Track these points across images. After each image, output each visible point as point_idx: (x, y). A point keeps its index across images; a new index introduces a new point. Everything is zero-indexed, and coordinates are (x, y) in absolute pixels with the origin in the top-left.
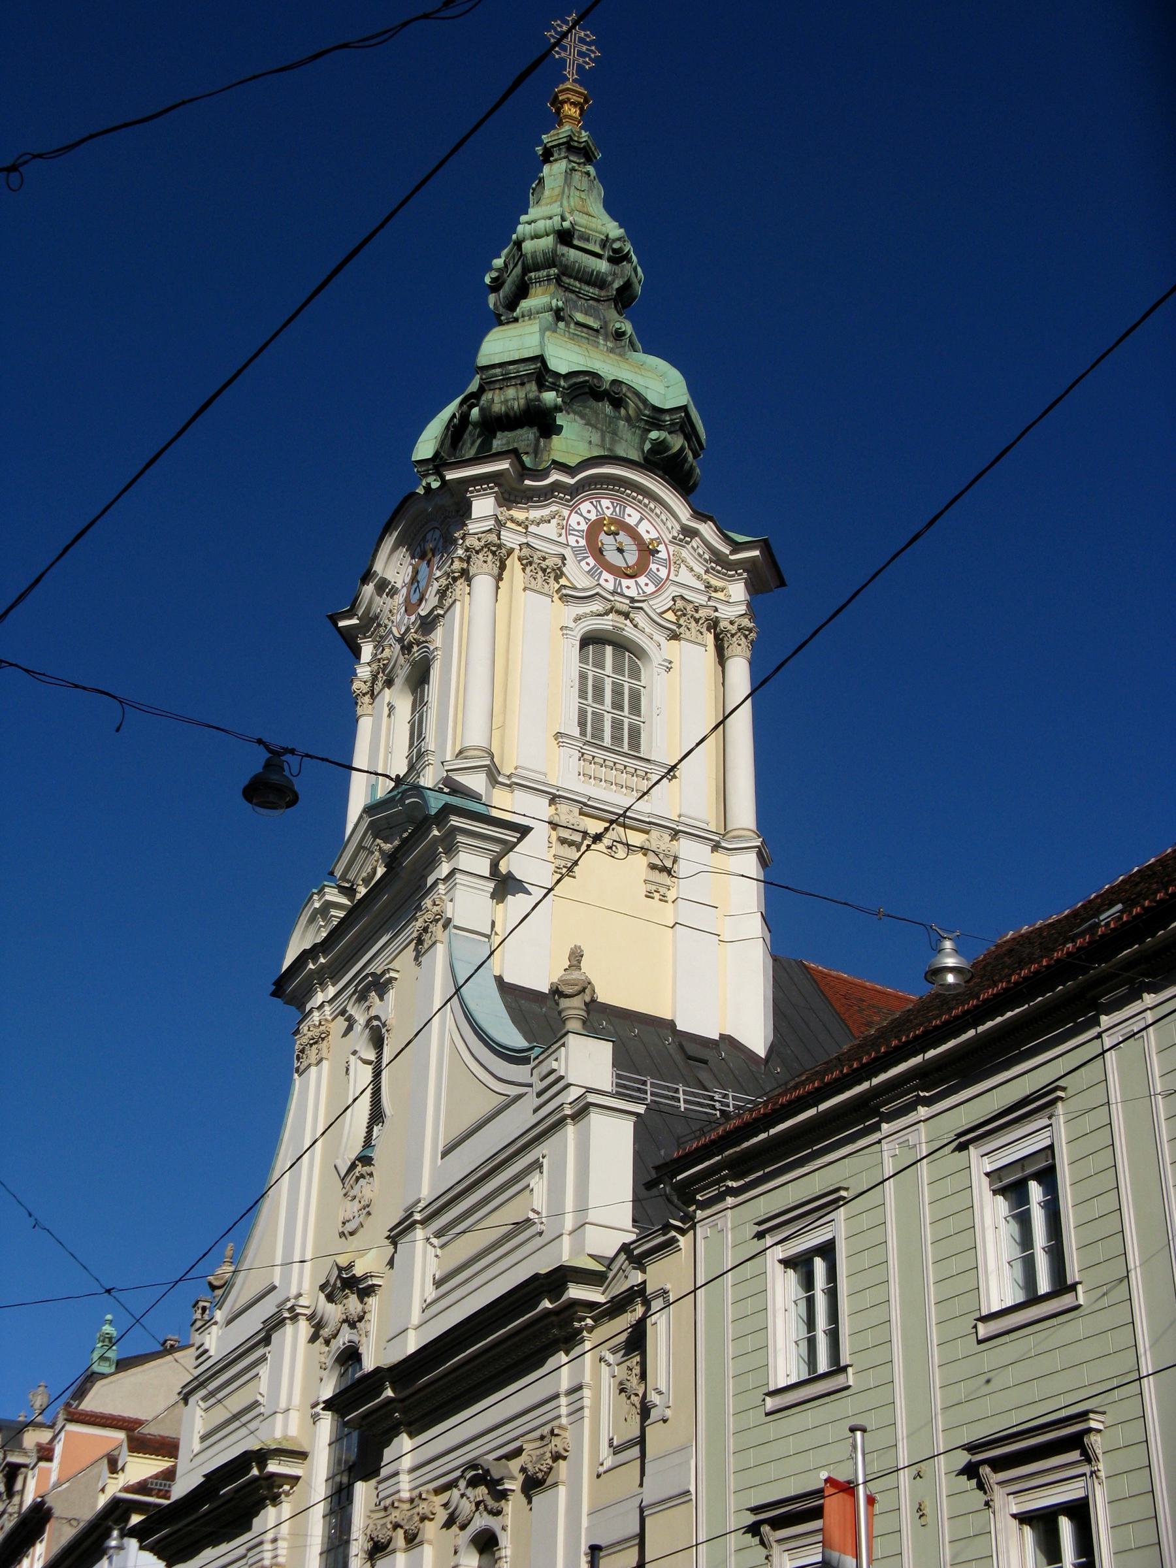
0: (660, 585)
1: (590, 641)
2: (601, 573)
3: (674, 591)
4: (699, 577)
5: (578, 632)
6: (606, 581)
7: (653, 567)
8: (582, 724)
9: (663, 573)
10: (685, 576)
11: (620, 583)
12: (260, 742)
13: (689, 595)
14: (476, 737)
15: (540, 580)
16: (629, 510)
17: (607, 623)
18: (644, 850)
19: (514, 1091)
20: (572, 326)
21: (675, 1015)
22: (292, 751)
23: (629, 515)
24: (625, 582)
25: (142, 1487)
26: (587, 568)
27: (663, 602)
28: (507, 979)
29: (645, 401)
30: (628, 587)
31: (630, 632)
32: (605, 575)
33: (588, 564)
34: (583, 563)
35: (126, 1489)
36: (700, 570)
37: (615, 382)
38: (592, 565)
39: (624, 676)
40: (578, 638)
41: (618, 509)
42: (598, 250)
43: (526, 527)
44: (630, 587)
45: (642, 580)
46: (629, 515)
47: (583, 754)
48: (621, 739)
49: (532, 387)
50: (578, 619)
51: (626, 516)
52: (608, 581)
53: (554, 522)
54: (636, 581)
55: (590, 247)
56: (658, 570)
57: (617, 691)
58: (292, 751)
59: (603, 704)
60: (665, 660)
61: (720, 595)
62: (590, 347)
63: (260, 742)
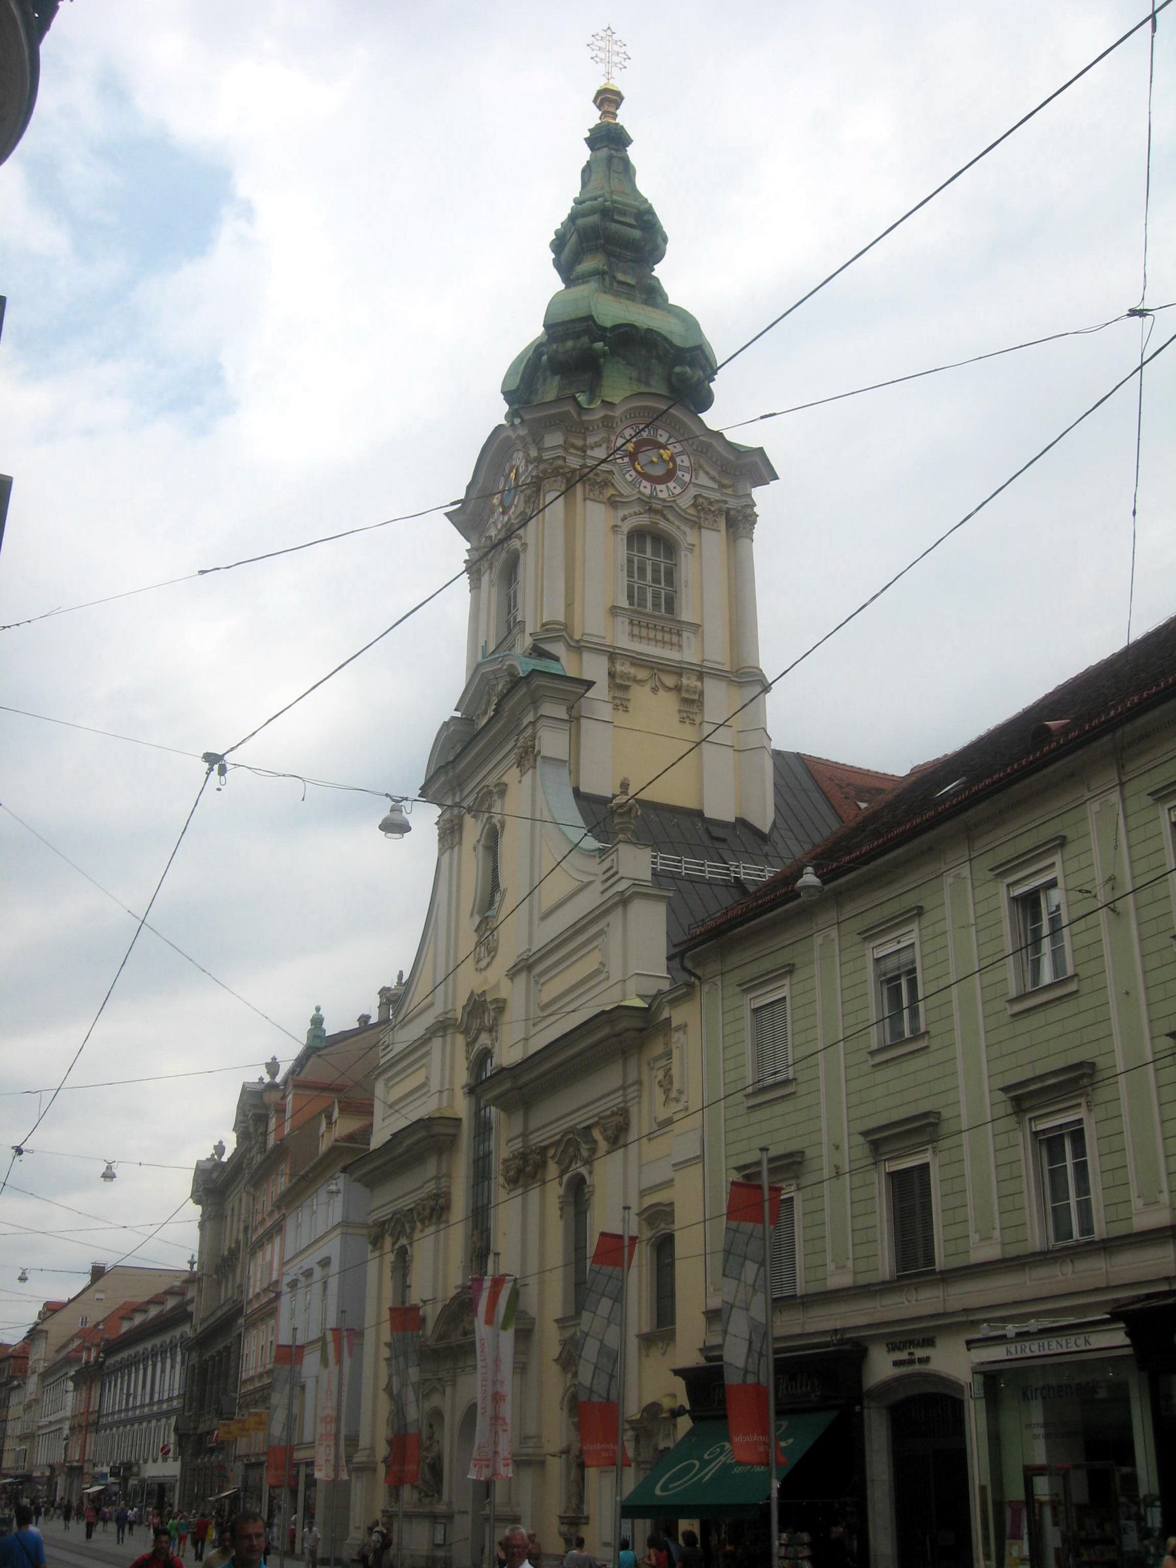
0: (685, 487)
2: (641, 481)
4: (713, 479)
5: (626, 527)
6: (645, 487)
7: (679, 473)
8: (630, 597)
9: (687, 478)
10: (703, 479)
11: (655, 488)
12: (387, 795)
13: (706, 493)
14: (555, 611)
15: (597, 492)
16: (660, 432)
17: (644, 520)
18: (678, 688)
19: (586, 879)
20: (615, 284)
22: (406, 799)
23: (661, 435)
24: (659, 487)
25: (351, 1138)
26: (630, 479)
27: (685, 502)
28: (583, 789)
29: (670, 343)
30: (661, 491)
31: (663, 524)
32: (644, 483)
33: (631, 476)
34: (627, 476)
35: (336, 1140)
36: (713, 473)
37: (650, 331)
38: (634, 476)
39: (660, 558)
40: (626, 533)
41: (652, 432)
42: (633, 222)
43: (585, 452)
44: (662, 491)
45: (672, 484)
46: (661, 435)
47: (632, 620)
48: (660, 605)
49: (585, 340)
50: (624, 519)
51: (658, 436)
52: (646, 488)
53: (604, 446)
54: (667, 486)
56: (683, 476)
57: (656, 571)
58: (406, 799)
59: (645, 580)
60: (690, 544)
61: (729, 491)
62: (628, 302)
63: (387, 795)
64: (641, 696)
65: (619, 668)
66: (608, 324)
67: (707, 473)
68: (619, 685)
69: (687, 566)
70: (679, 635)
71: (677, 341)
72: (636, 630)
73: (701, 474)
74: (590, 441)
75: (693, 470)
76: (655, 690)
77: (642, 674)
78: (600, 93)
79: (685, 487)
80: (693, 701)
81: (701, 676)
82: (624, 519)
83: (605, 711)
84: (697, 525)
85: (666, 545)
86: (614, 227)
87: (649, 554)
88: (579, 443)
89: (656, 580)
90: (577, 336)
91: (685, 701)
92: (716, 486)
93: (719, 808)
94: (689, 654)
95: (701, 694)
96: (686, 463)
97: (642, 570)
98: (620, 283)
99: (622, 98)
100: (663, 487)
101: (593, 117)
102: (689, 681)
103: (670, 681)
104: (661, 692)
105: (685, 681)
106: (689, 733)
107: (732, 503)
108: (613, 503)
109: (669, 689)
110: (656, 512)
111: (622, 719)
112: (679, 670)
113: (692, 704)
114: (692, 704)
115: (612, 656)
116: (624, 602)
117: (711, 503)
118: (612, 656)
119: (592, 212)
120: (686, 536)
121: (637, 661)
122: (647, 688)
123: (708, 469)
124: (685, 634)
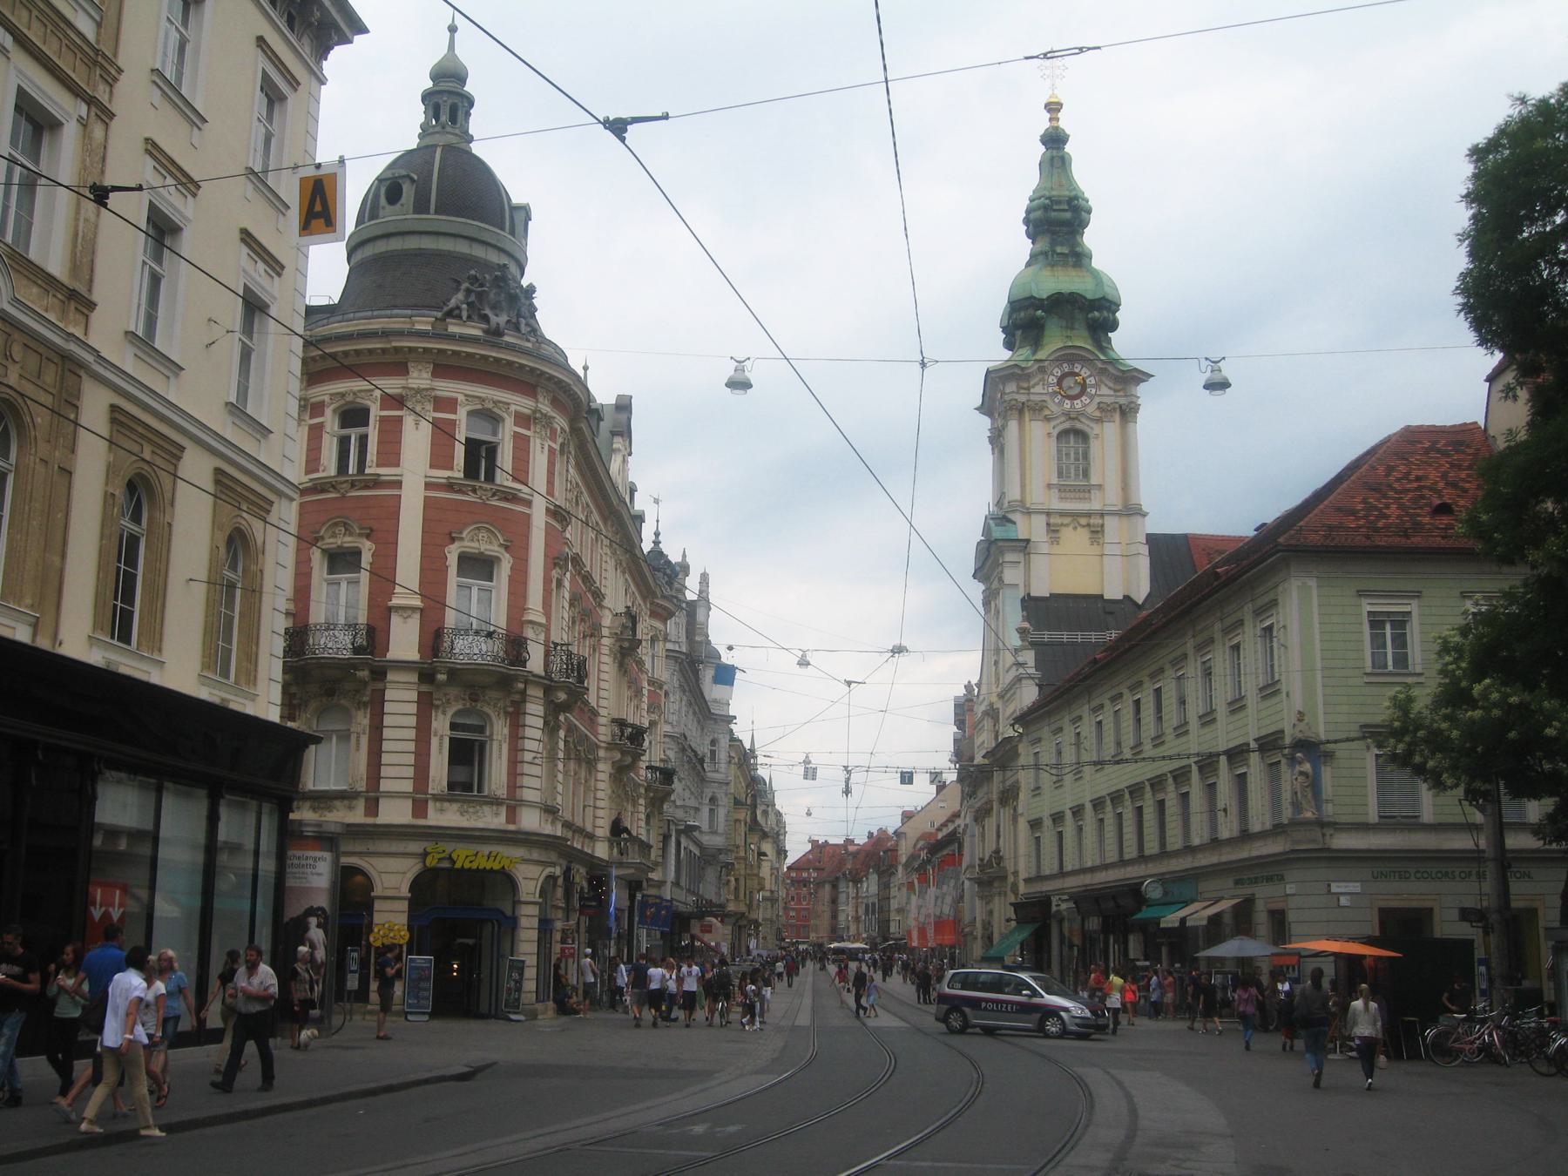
0: (1092, 397)
1: (1063, 435)
3: (1097, 400)
4: (1110, 388)
10: (1105, 390)
13: (1105, 400)
17: (1067, 425)
21: (1103, 590)
24: (1075, 402)
27: (1092, 410)
29: (1085, 298)
31: (1079, 426)
32: (1067, 401)
36: (1111, 385)
42: (1066, 207)
44: (1078, 404)
50: (1054, 428)
52: (1067, 404)
55: (1062, 207)
57: (1076, 453)
61: (1121, 393)
64: (1067, 534)
65: (1052, 521)
66: (1045, 297)
67: (1106, 385)
68: (1053, 530)
69: (1095, 446)
70: (1089, 492)
71: (1089, 296)
72: (1063, 495)
73: (1103, 386)
74: (1032, 383)
75: (1097, 386)
76: (1075, 528)
77: (1066, 520)
78: (1046, 106)
79: (1092, 397)
80: (1098, 532)
81: (1102, 515)
82: (1054, 428)
83: (1045, 548)
84: (1099, 420)
85: (1082, 436)
86: (1053, 214)
87: (1072, 444)
88: (1025, 385)
89: (1077, 459)
90: (1026, 308)
91: (1093, 532)
92: (1112, 393)
93: (1113, 592)
94: (1095, 505)
95: (1102, 526)
96: (1093, 382)
97: (1068, 455)
98: (1058, 254)
99: (1061, 105)
100: (1078, 401)
101: (1042, 123)
102: (1096, 521)
103: (1083, 521)
104: (1079, 529)
105: (1092, 521)
106: (1096, 549)
107: (1122, 401)
108: (1047, 419)
109: (1084, 526)
110: (1073, 419)
111: (1056, 549)
112: (1089, 515)
113: (1097, 533)
114: (1097, 533)
115: (1048, 514)
116: (1055, 481)
117: (1108, 405)
118: (1048, 514)
119: (1039, 208)
120: (1094, 429)
121: (1062, 514)
122: (1071, 528)
123: (1107, 382)
124: (1092, 492)
